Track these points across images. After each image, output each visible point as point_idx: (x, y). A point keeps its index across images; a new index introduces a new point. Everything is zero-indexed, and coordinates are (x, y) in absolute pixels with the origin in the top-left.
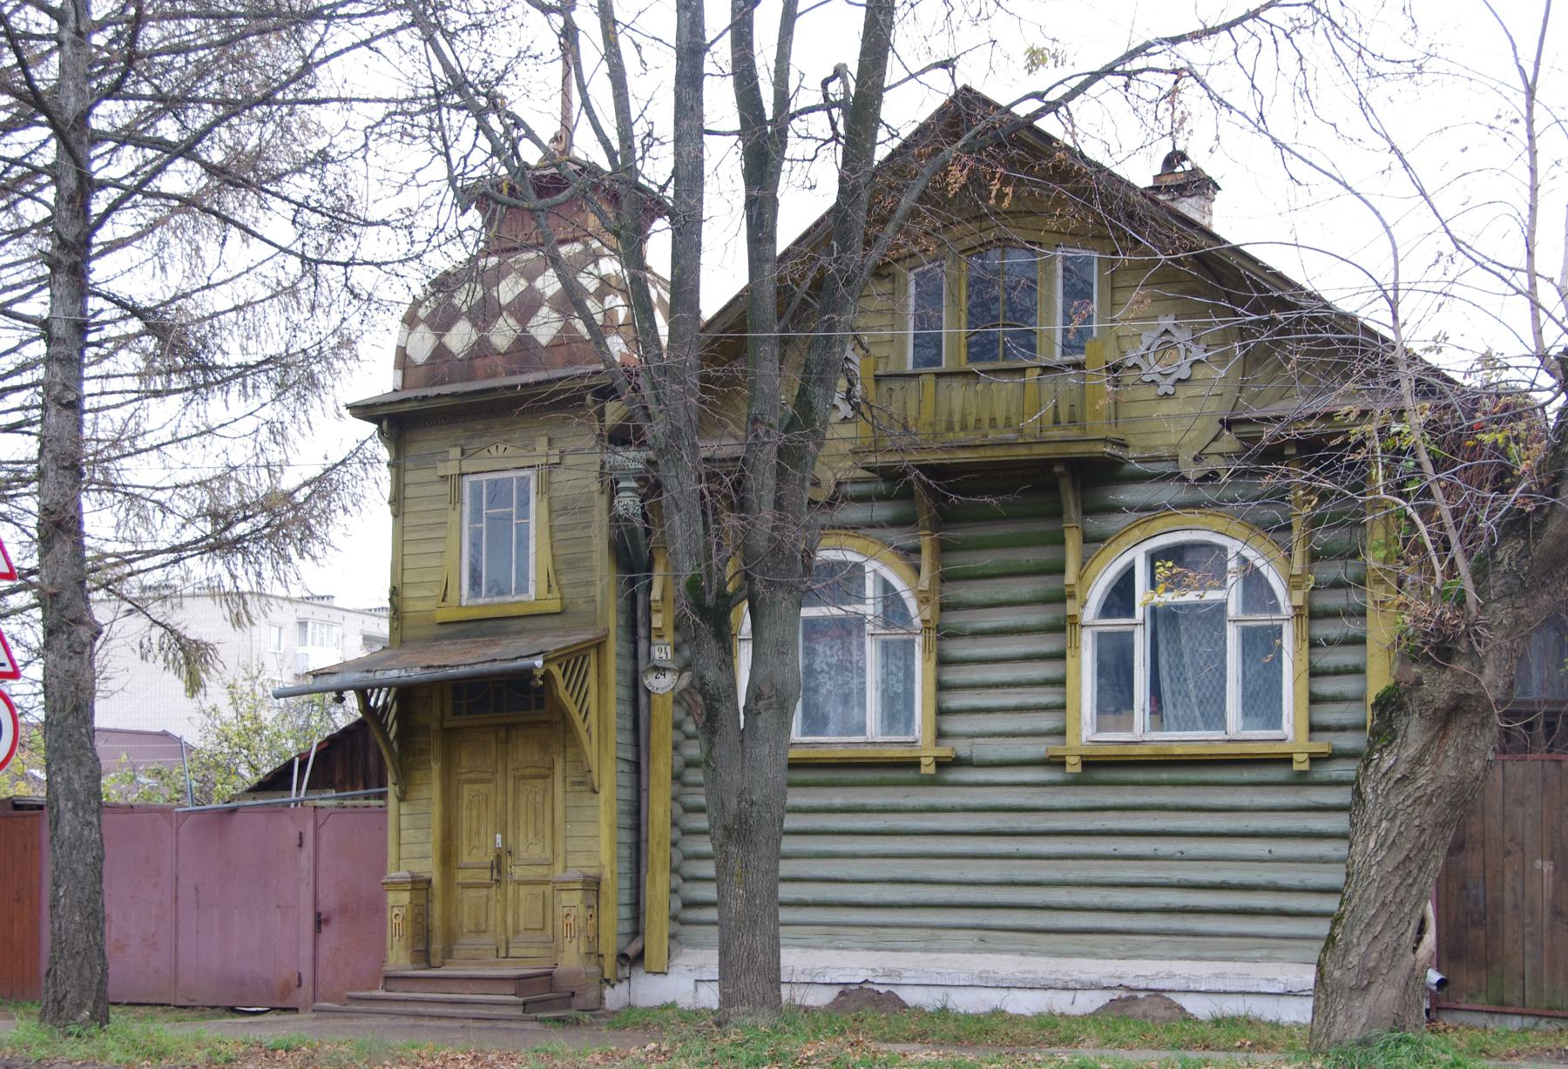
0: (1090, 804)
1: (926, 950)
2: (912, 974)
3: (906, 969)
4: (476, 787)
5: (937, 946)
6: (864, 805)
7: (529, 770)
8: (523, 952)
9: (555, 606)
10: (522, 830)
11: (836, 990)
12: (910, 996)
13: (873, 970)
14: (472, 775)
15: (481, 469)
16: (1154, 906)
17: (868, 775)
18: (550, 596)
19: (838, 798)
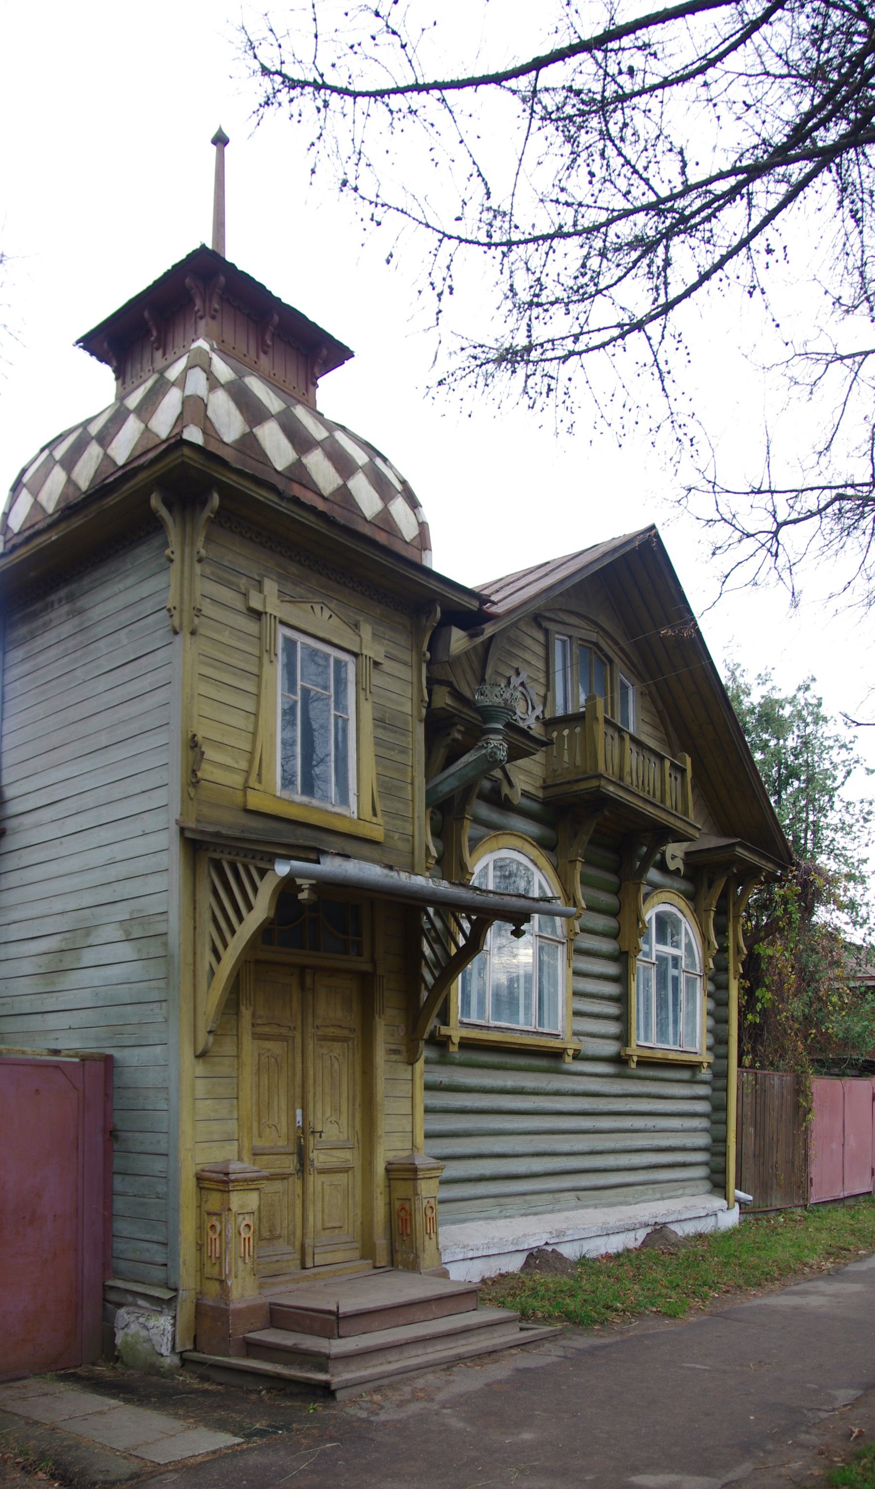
0: (625, 1092)
1: (552, 1212)
2: (570, 1232)
3: (568, 1229)
4: (268, 1045)
5: (558, 1207)
6: (523, 1088)
7: (332, 1029)
8: (330, 1258)
9: (377, 834)
10: (319, 1105)
11: (526, 1254)
12: (569, 1251)
13: (551, 1233)
14: (266, 1029)
15: (303, 626)
16: (643, 1165)
17: (522, 1061)
18: (374, 820)
19: (509, 1080)
